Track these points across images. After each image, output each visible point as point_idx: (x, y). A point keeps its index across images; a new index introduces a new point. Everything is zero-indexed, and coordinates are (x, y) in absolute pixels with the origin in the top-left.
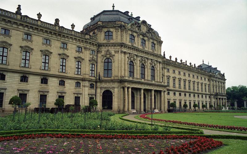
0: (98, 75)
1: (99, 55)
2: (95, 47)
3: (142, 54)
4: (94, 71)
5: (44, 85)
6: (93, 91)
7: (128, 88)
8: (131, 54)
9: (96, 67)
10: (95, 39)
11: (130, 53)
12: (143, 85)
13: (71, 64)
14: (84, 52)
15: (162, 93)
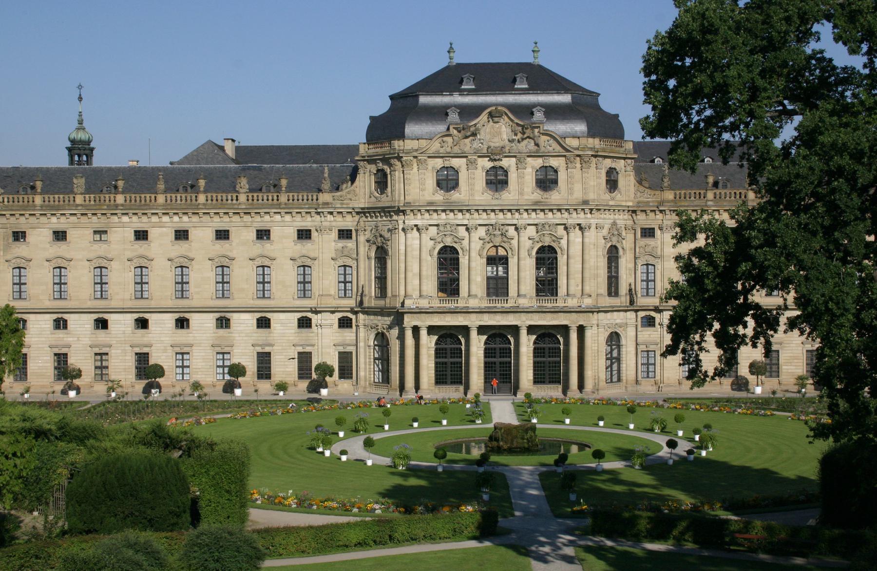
0: (359, 294)
1: (362, 239)
2: (349, 217)
3: (489, 219)
4: (351, 282)
5: (222, 332)
6: (348, 335)
7: (416, 330)
8: (441, 228)
9: (355, 273)
10: (349, 196)
11: (437, 225)
12: (473, 316)
13: (284, 278)
14: (317, 240)
15: (574, 336)
